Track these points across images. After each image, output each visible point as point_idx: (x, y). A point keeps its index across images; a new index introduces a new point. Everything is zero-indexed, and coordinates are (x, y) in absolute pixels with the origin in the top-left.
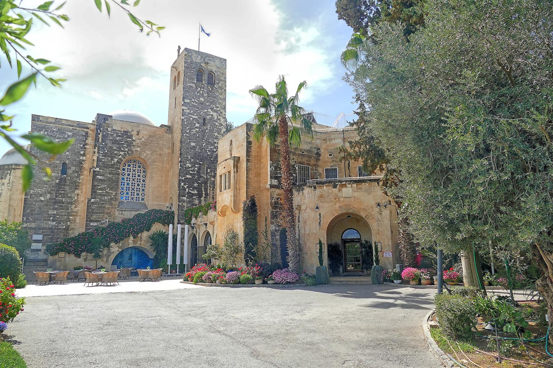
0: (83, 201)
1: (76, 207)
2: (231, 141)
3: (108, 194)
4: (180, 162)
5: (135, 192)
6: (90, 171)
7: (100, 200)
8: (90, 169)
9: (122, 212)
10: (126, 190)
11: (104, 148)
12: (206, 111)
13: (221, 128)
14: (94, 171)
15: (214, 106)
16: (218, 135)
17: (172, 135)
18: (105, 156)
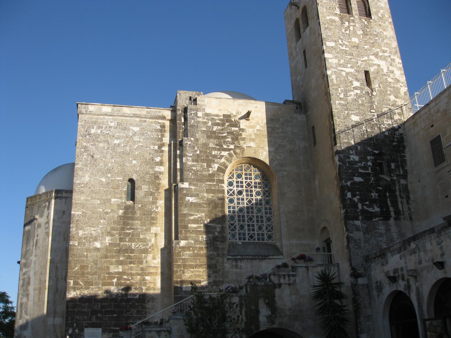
5: (255, 223)
9: (236, 262)
10: (239, 221)
11: (194, 147)
12: (366, 58)
13: (399, 86)
15: (378, 50)
16: (396, 99)
18: (197, 161)
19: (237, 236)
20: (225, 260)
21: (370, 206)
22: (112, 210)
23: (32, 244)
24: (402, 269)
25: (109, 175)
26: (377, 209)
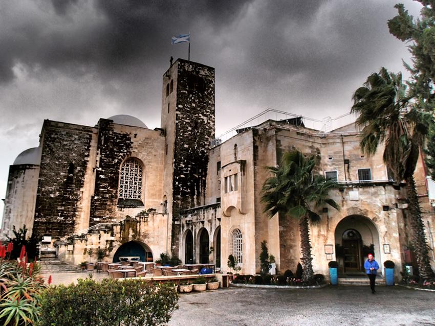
0: (87, 198)
1: (81, 204)
2: (236, 145)
3: (109, 192)
4: (175, 163)
5: (133, 190)
6: (94, 171)
7: (103, 197)
8: (94, 169)
10: (125, 188)
12: (197, 115)
14: (97, 171)
17: (166, 138)
19: (123, 195)
20: (116, 207)
21: (186, 189)
22: (61, 179)
23: (13, 191)
24: (191, 221)
25: (60, 160)
26: (189, 191)
